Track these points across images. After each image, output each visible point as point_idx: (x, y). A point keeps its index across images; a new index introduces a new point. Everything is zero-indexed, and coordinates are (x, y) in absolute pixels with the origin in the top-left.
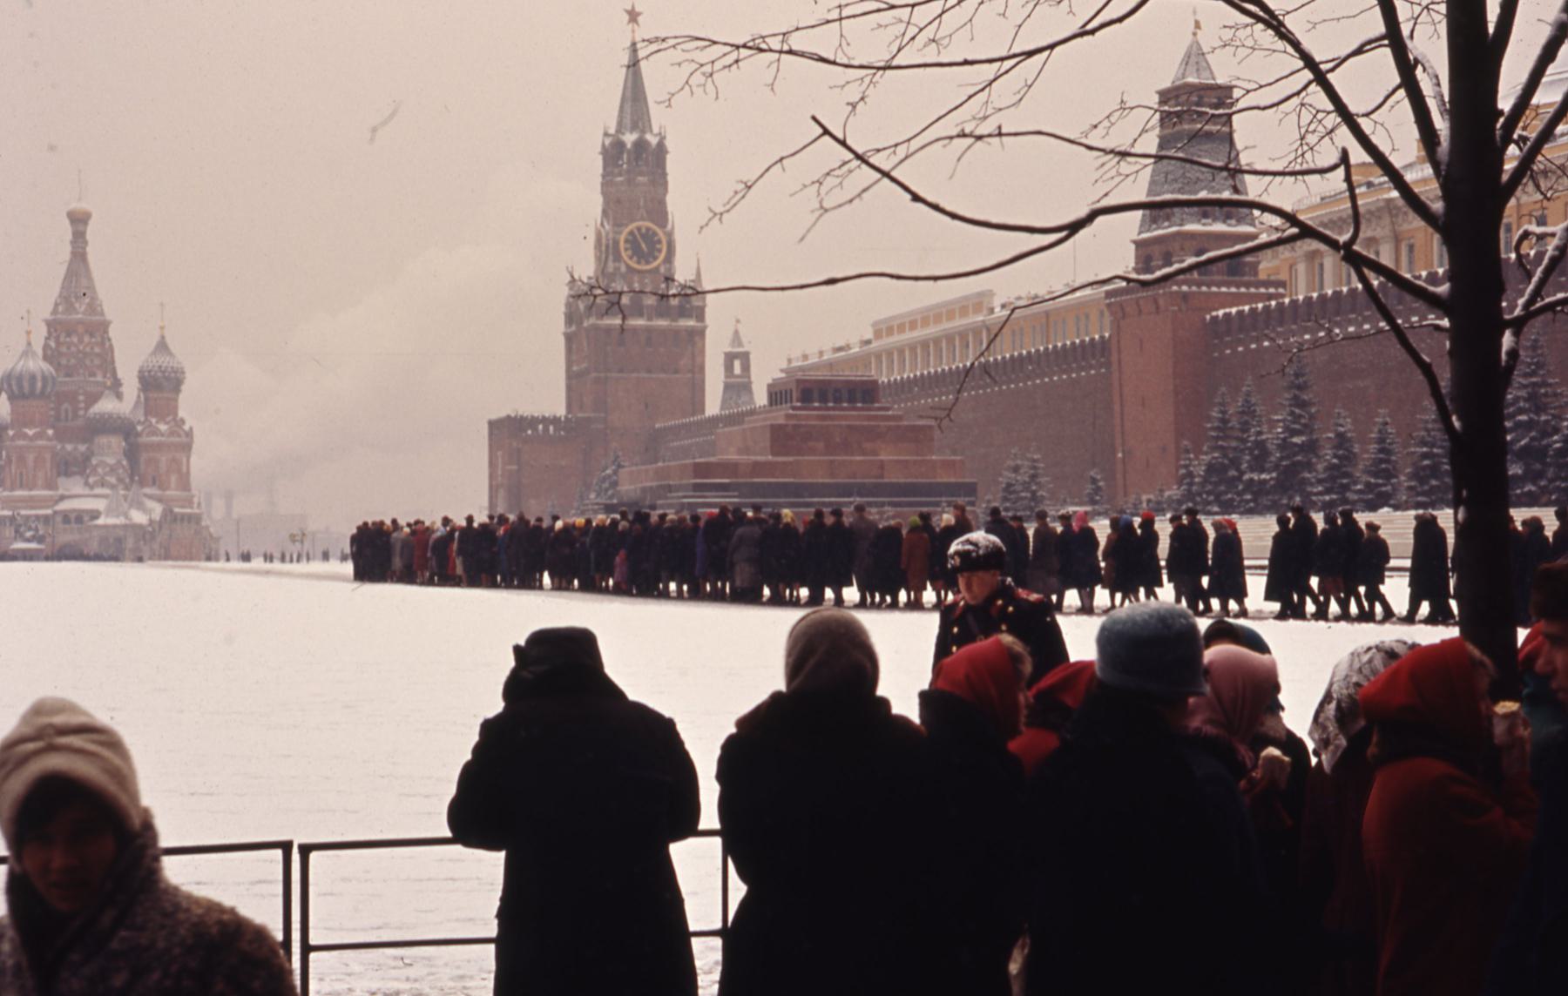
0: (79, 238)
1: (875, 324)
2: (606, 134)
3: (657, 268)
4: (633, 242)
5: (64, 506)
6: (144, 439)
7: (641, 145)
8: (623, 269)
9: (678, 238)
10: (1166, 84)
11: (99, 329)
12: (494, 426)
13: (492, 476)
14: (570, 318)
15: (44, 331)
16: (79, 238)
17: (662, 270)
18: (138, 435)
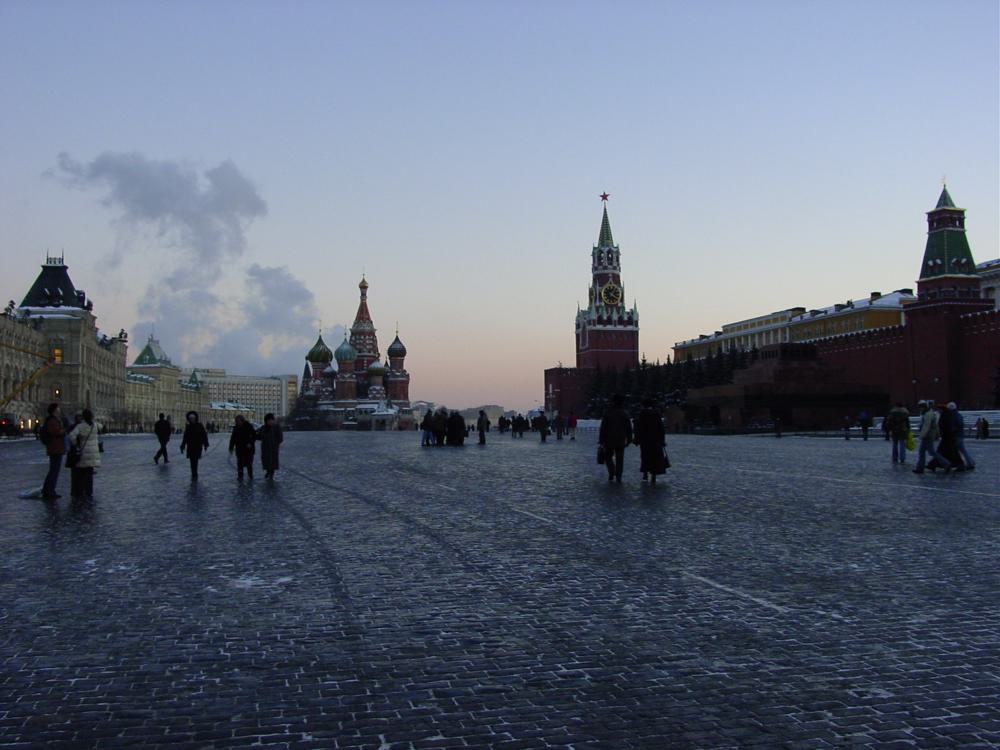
0: (363, 295)
1: (724, 327)
2: (594, 248)
4: (607, 292)
5: (359, 407)
6: (391, 379)
7: (609, 252)
8: (603, 304)
9: (625, 290)
10: (932, 207)
11: (372, 333)
12: (546, 371)
13: (547, 394)
14: (578, 326)
16: (363, 295)
17: (620, 304)
18: (388, 377)
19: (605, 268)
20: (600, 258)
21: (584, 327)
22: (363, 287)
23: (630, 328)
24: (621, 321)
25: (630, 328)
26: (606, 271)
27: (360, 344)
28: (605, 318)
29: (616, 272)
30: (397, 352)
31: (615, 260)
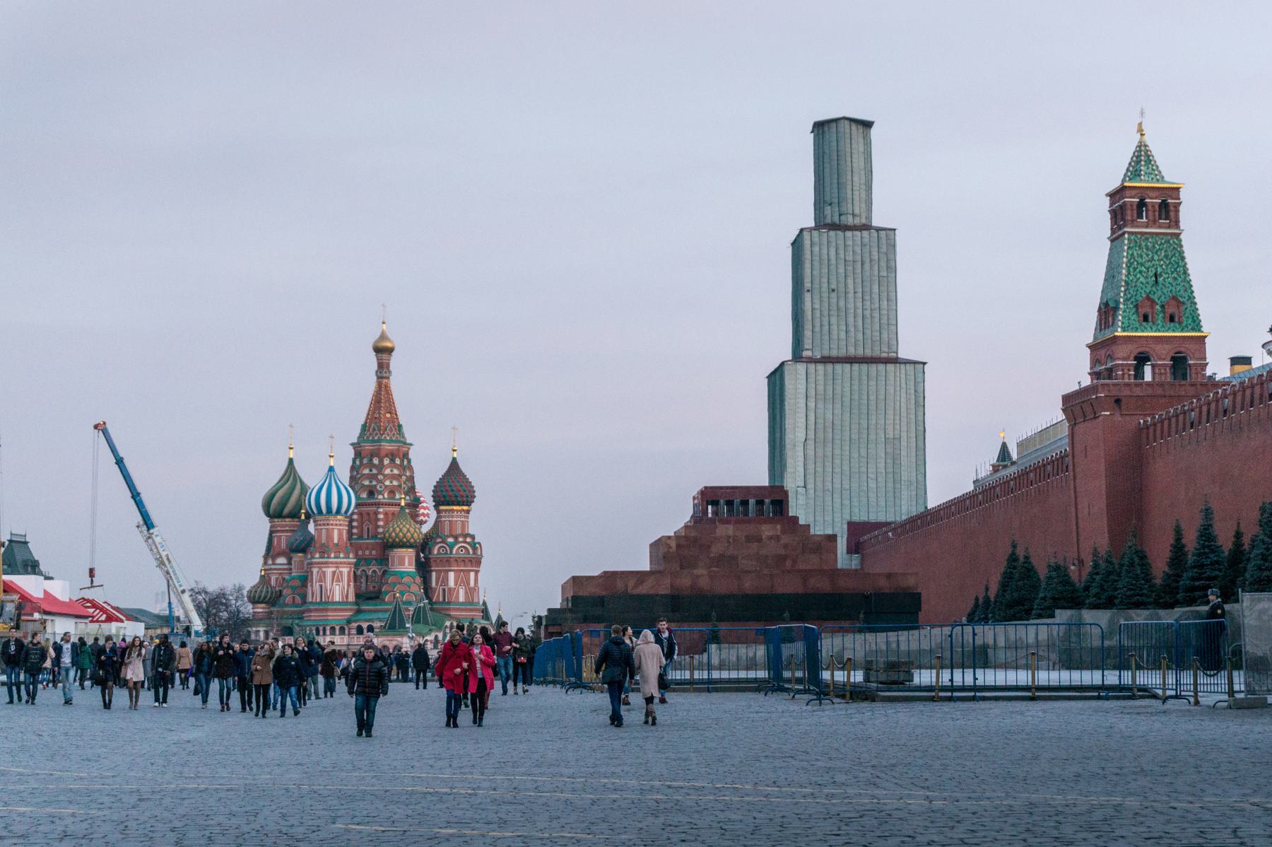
15: (351, 453)
22: (383, 351)
27: (372, 477)
30: (455, 490)
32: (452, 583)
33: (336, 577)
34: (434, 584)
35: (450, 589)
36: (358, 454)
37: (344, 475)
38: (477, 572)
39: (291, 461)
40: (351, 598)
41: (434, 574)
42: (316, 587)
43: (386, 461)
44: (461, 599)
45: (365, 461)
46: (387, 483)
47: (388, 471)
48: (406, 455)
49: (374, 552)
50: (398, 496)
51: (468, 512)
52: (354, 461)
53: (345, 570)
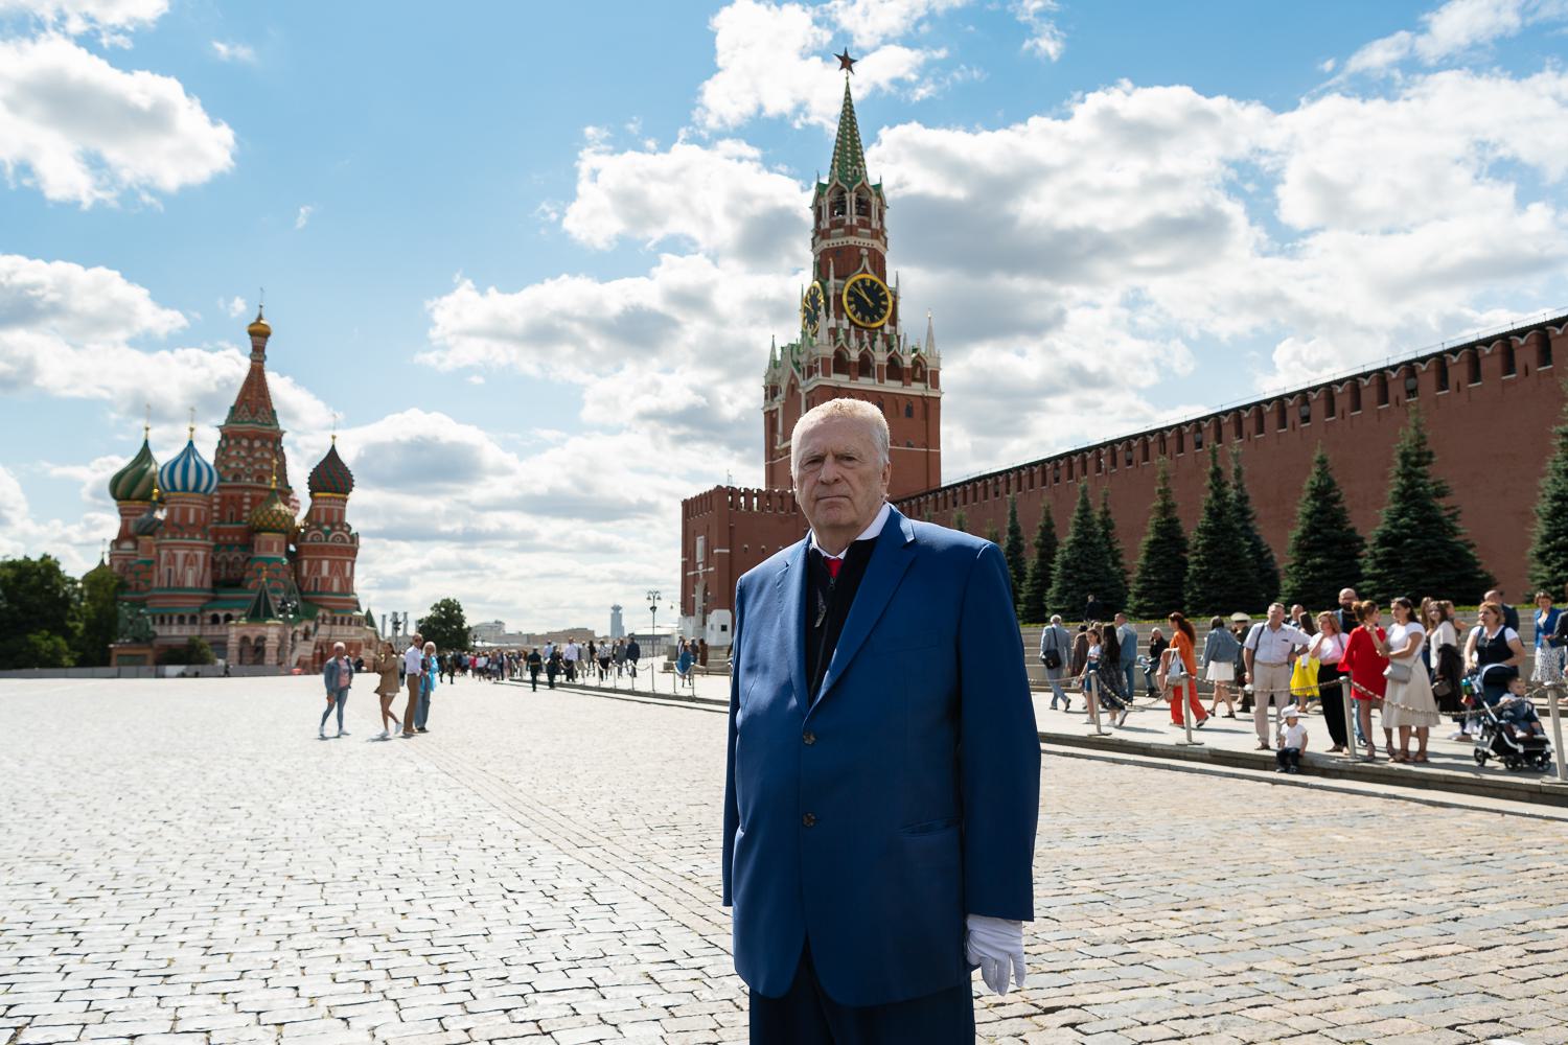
0: (258, 354)
3: (882, 327)
8: (845, 324)
11: (273, 440)
12: (686, 504)
13: (685, 567)
17: (888, 329)
19: (851, 231)
20: (839, 205)
21: (793, 388)
23: (917, 389)
24: (894, 370)
25: (917, 389)
26: (852, 240)
28: (854, 355)
29: (876, 244)
30: (332, 477)
31: (874, 213)
32: (325, 572)
33: (189, 561)
34: (305, 573)
35: (324, 580)
36: (224, 436)
37: (208, 453)
38: (353, 563)
39: (146, 443)
40: (207, 584)
41: (305, 563)
42: (164, 569)
43: (257, 444)
44: (336, 588)
45: (232, 442)
46: (257, 467)
47: (258, 455)
48: (278, 440)
49: (237, 538)
50: (268, 481)
51: (346, 500)
52: (220, 443)
53: (201, 553)
